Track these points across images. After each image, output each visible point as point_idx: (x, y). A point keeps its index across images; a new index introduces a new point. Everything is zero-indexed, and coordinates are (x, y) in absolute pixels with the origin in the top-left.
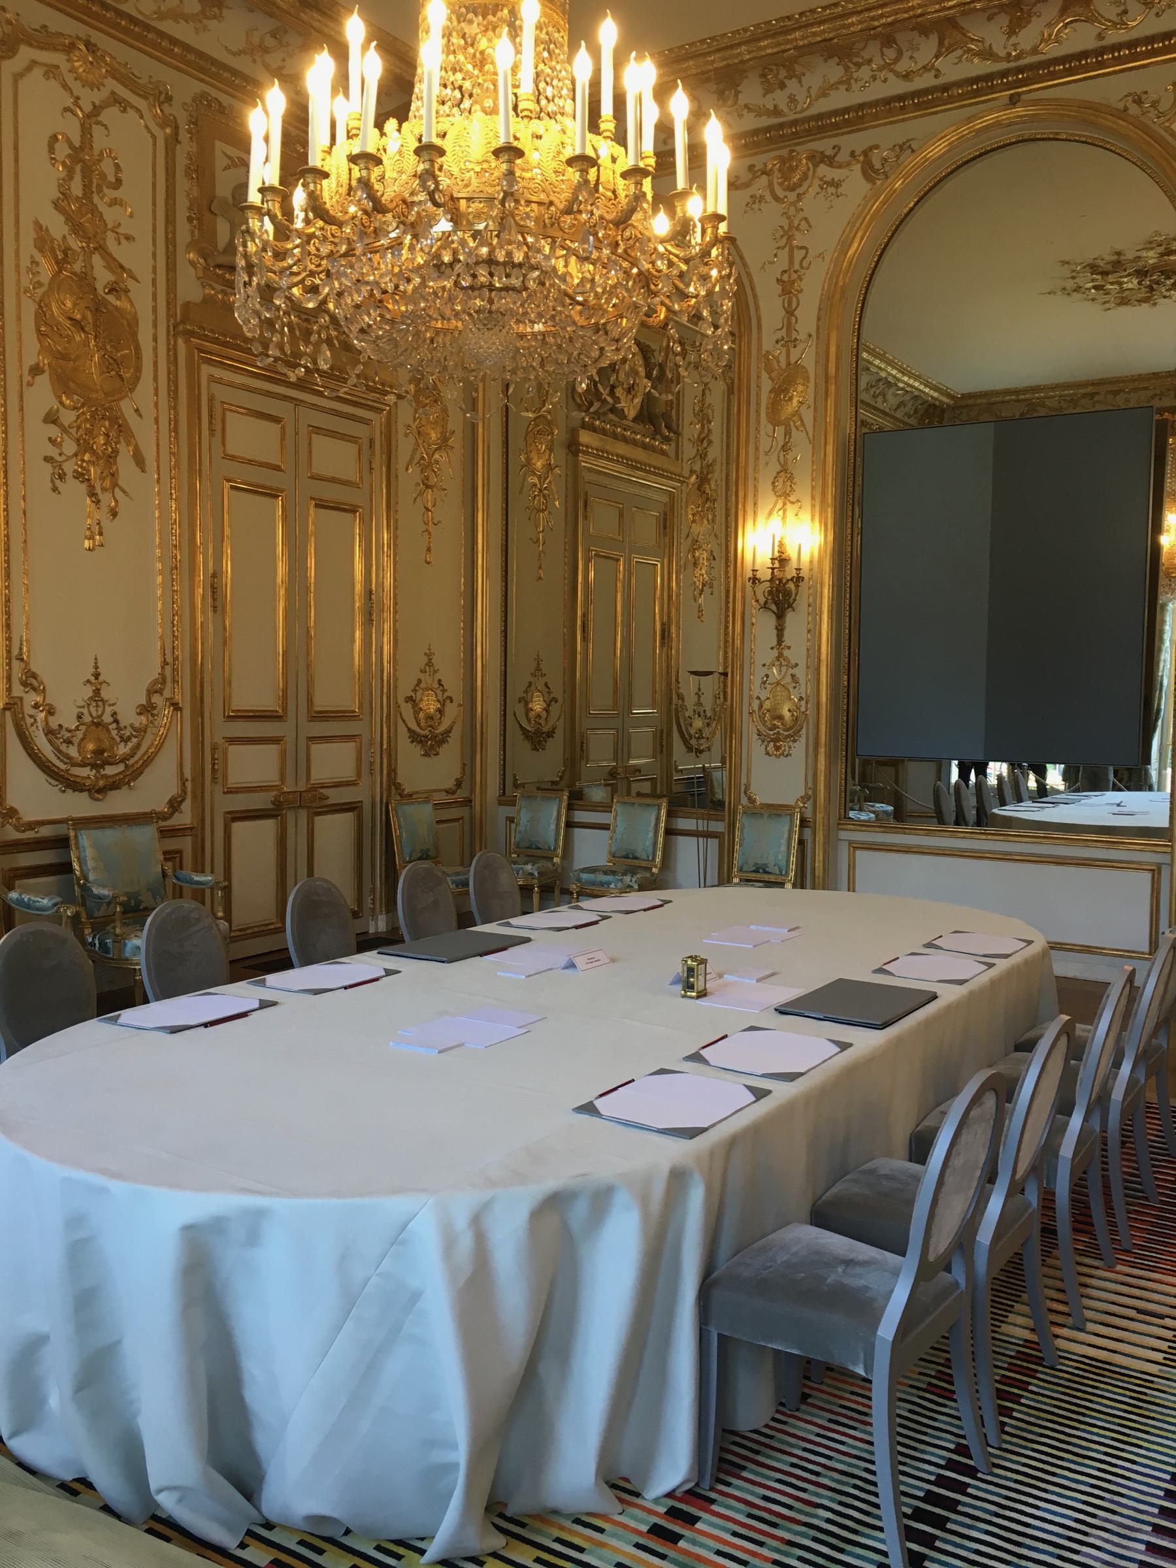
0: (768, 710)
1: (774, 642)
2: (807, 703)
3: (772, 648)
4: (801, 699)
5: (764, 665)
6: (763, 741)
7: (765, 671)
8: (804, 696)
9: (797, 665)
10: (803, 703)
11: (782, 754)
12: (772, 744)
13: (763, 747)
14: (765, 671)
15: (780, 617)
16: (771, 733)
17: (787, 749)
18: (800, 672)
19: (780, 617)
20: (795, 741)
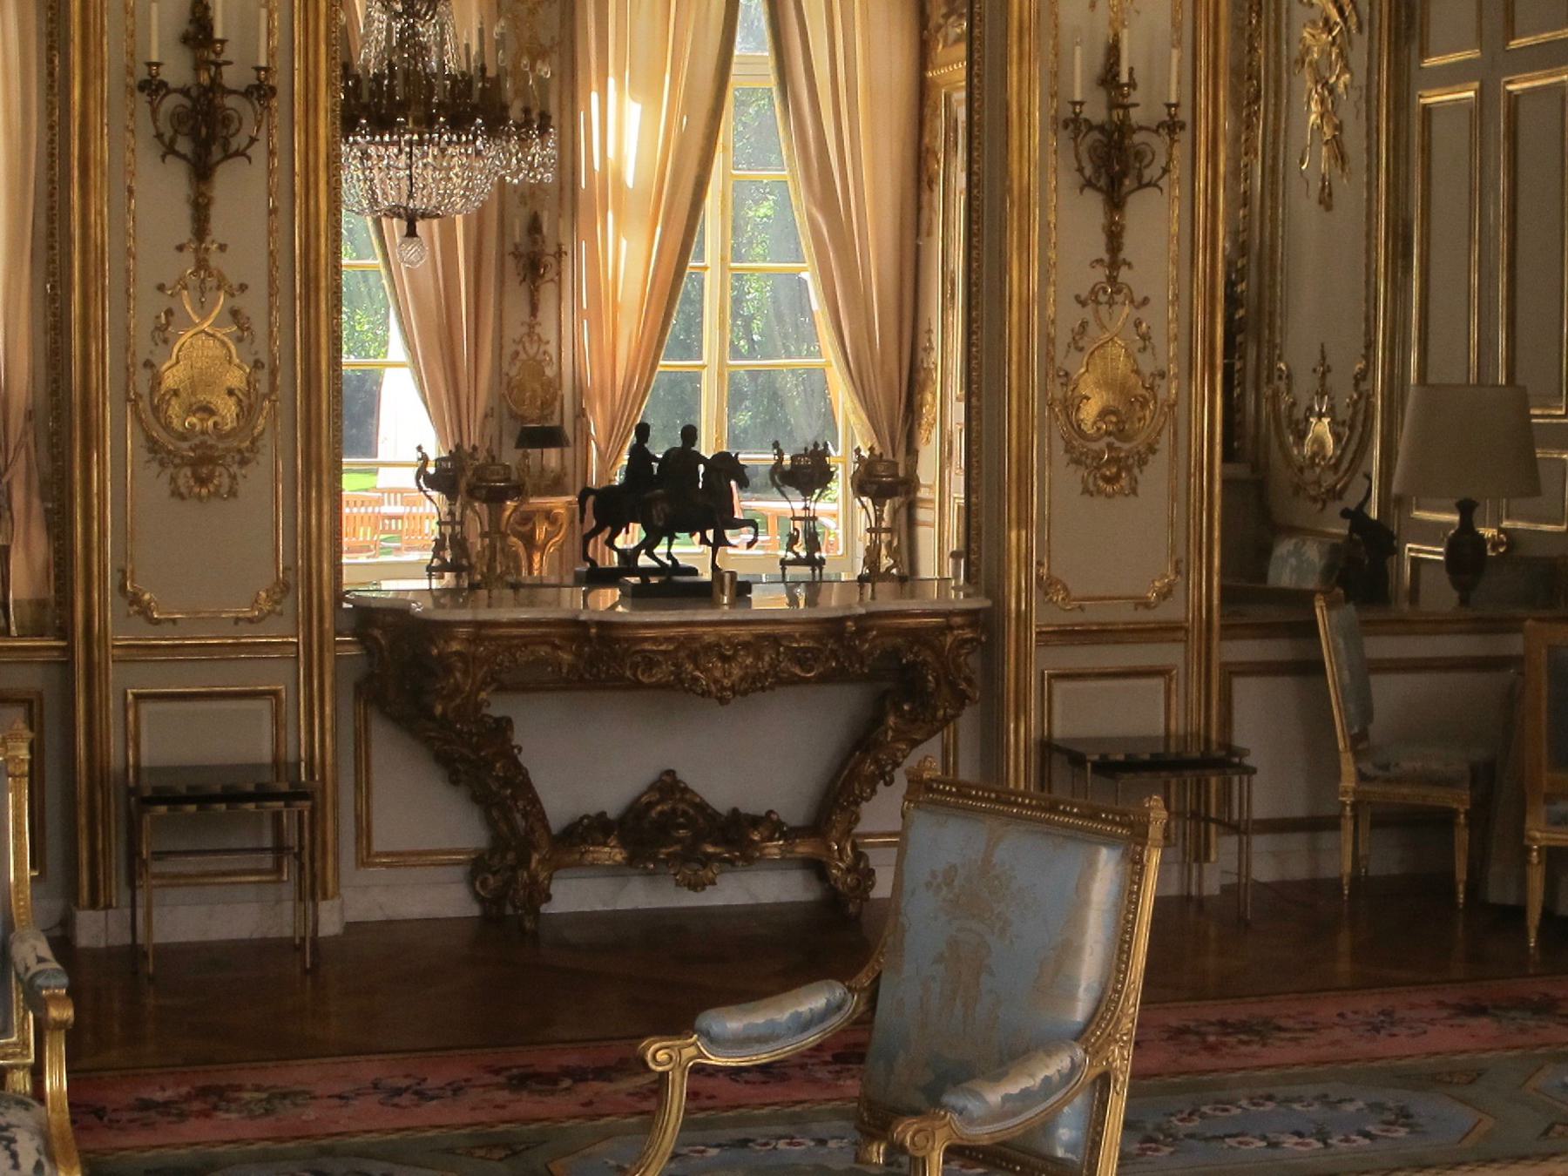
0: (176, 393)
1: (185, 233)
2: (273, 373)
3: (180, 248)
4: (257, 365)
5: (161, 288)
6: (162, 464)
7: (164, 302)
8: (264, 358)
9: (243, 287)
10: (263, 375)
11: (216, 494)
12: (188, 471)
13: (165, 478)
14: (164, 302)
15: (202, 172)
16: (185, 445)
17: (226, 480)
18: (254, 304)
19: (202, 172)
20: (243, 462)
